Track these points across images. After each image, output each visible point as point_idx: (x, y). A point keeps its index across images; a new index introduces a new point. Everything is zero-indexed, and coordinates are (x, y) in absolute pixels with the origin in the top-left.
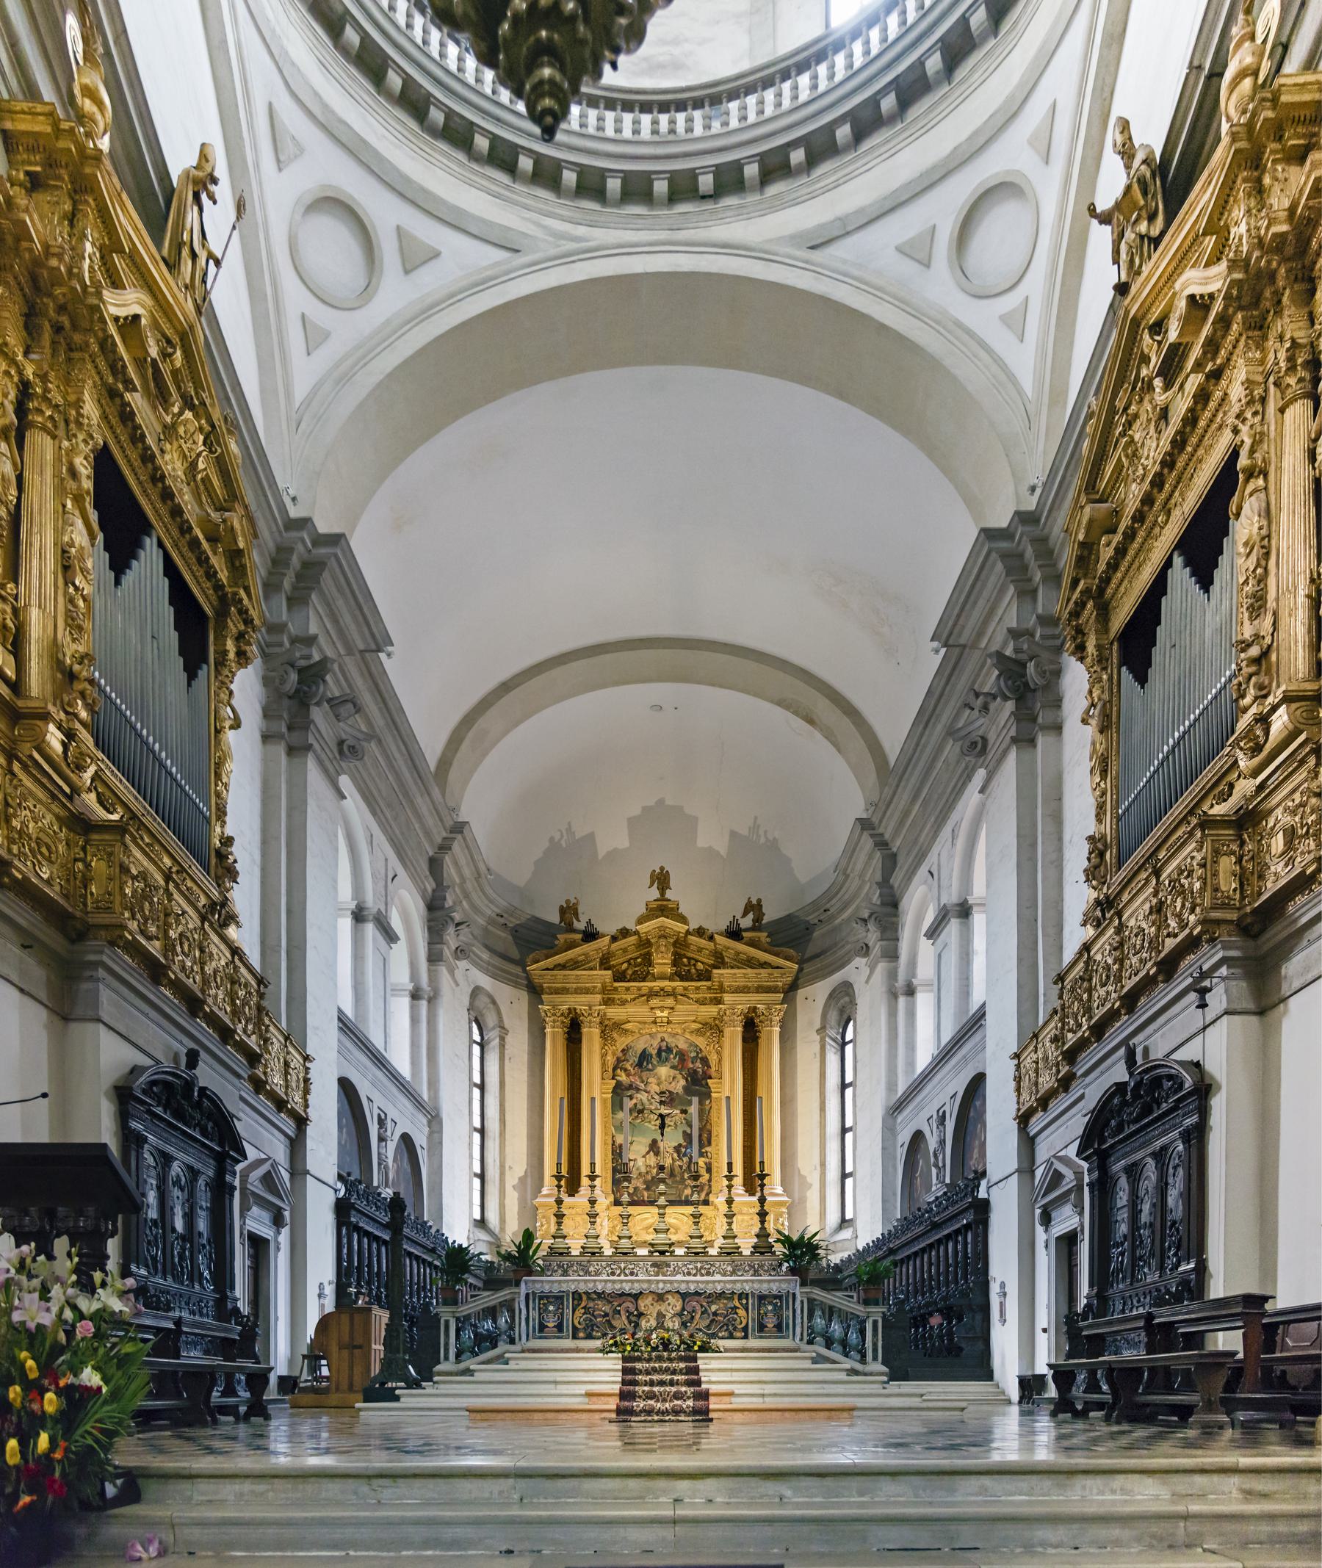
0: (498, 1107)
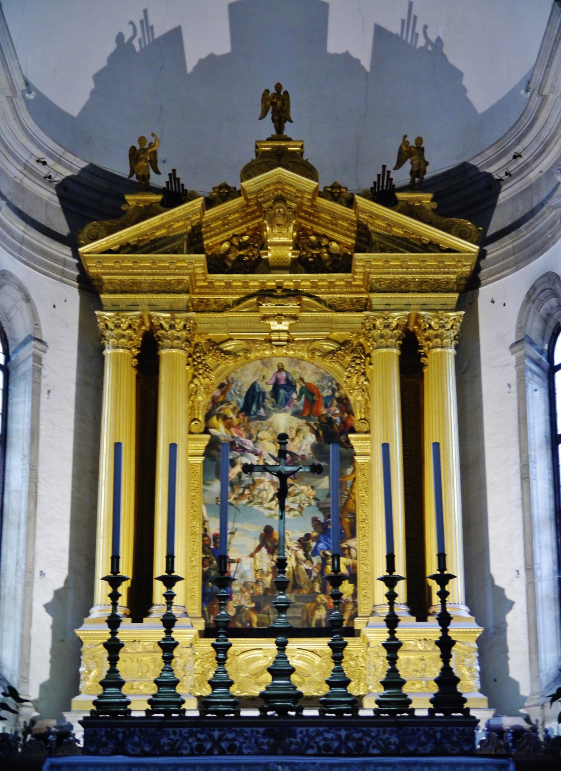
0: (26, 473)
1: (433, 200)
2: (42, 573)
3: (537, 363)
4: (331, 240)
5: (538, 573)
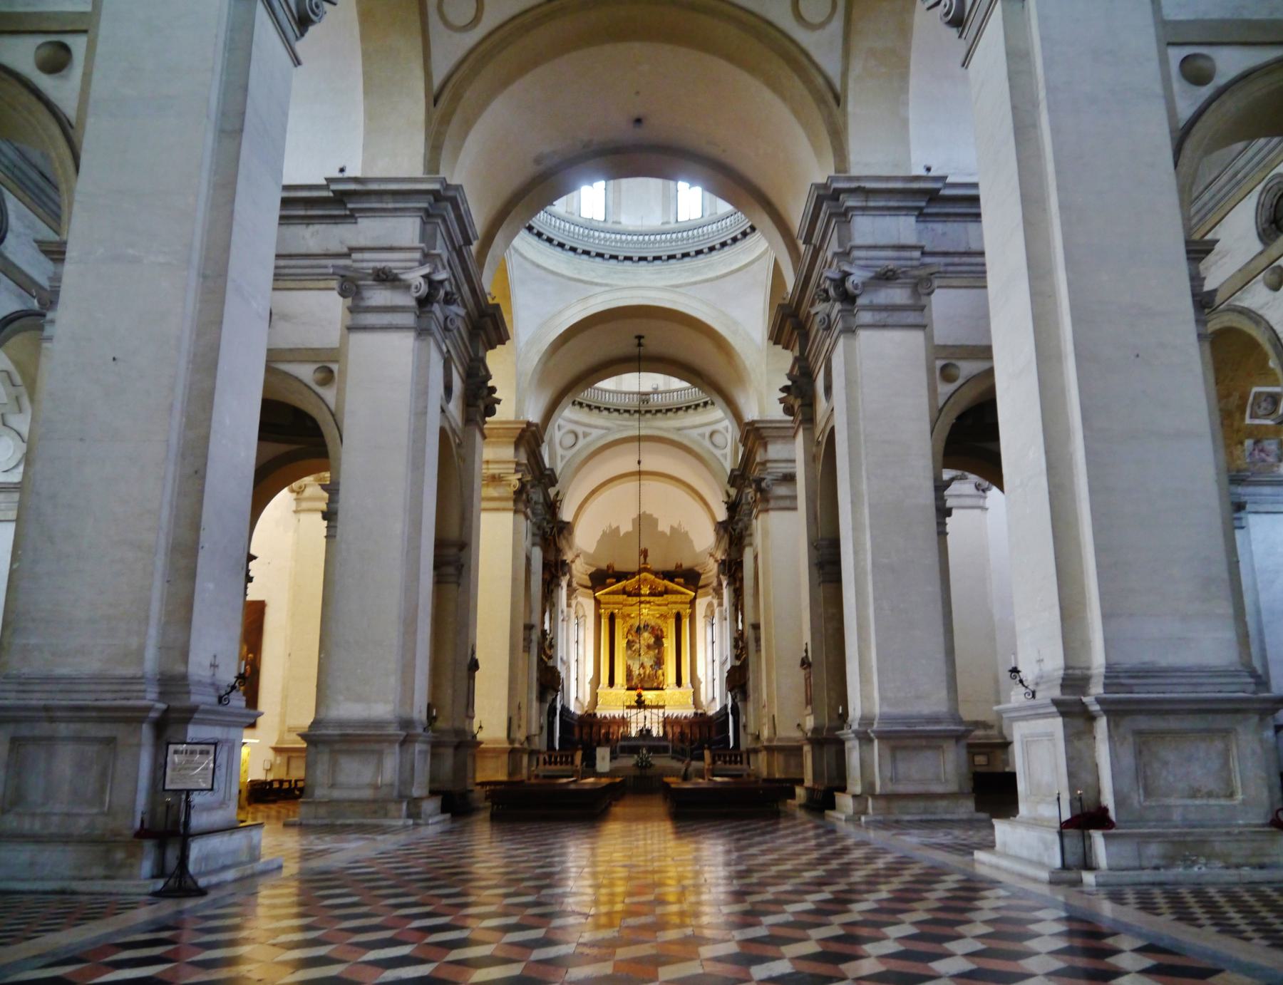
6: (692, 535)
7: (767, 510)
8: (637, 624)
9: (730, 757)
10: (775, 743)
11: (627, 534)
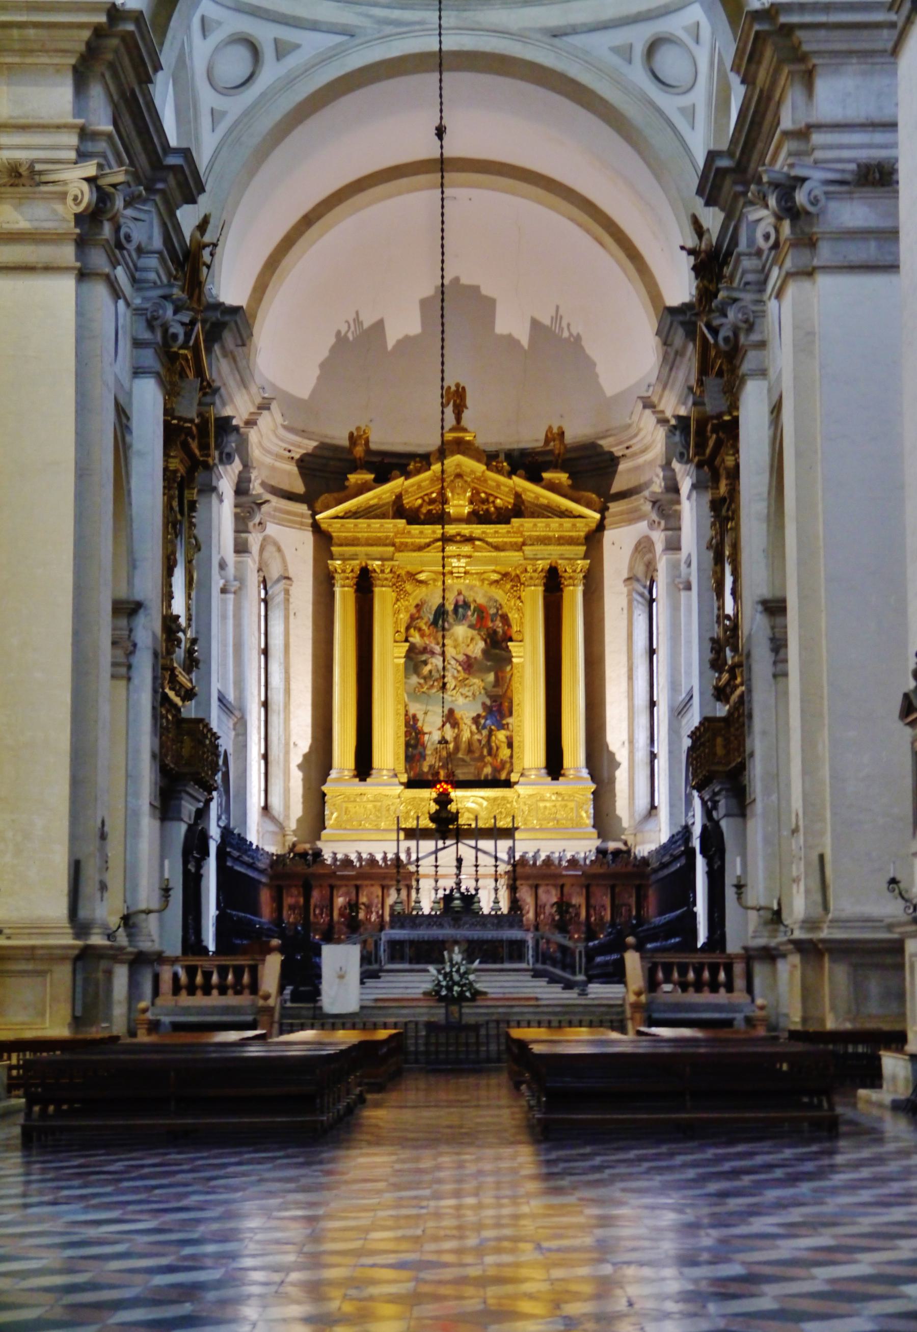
0: (283, 676)
1: (568, 478)
2: (295, 744)
3: (642, 595)
4: (496, 497)
5: (636, 745)
6: (592, 349)
7: (809, 273)
8: (436, 601)
9: (698, 972)
10: (825, 934)
11: (406, 342)
